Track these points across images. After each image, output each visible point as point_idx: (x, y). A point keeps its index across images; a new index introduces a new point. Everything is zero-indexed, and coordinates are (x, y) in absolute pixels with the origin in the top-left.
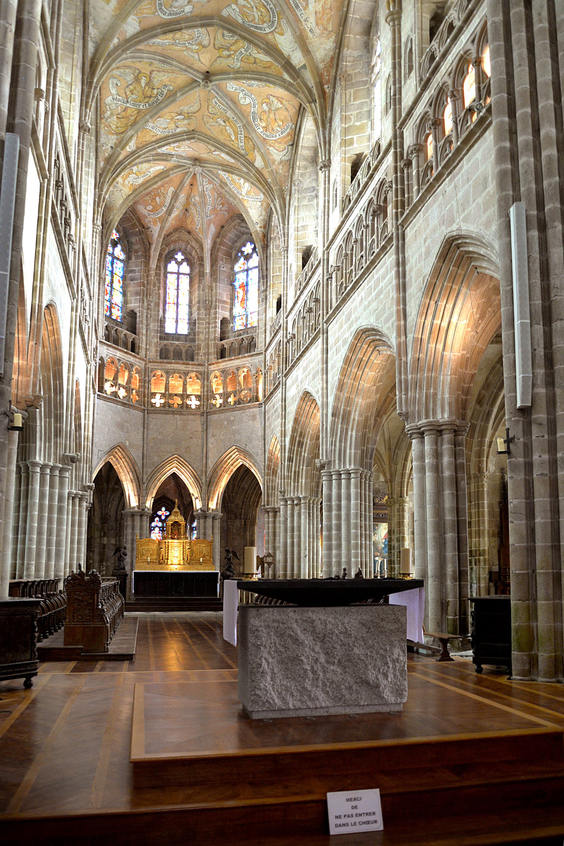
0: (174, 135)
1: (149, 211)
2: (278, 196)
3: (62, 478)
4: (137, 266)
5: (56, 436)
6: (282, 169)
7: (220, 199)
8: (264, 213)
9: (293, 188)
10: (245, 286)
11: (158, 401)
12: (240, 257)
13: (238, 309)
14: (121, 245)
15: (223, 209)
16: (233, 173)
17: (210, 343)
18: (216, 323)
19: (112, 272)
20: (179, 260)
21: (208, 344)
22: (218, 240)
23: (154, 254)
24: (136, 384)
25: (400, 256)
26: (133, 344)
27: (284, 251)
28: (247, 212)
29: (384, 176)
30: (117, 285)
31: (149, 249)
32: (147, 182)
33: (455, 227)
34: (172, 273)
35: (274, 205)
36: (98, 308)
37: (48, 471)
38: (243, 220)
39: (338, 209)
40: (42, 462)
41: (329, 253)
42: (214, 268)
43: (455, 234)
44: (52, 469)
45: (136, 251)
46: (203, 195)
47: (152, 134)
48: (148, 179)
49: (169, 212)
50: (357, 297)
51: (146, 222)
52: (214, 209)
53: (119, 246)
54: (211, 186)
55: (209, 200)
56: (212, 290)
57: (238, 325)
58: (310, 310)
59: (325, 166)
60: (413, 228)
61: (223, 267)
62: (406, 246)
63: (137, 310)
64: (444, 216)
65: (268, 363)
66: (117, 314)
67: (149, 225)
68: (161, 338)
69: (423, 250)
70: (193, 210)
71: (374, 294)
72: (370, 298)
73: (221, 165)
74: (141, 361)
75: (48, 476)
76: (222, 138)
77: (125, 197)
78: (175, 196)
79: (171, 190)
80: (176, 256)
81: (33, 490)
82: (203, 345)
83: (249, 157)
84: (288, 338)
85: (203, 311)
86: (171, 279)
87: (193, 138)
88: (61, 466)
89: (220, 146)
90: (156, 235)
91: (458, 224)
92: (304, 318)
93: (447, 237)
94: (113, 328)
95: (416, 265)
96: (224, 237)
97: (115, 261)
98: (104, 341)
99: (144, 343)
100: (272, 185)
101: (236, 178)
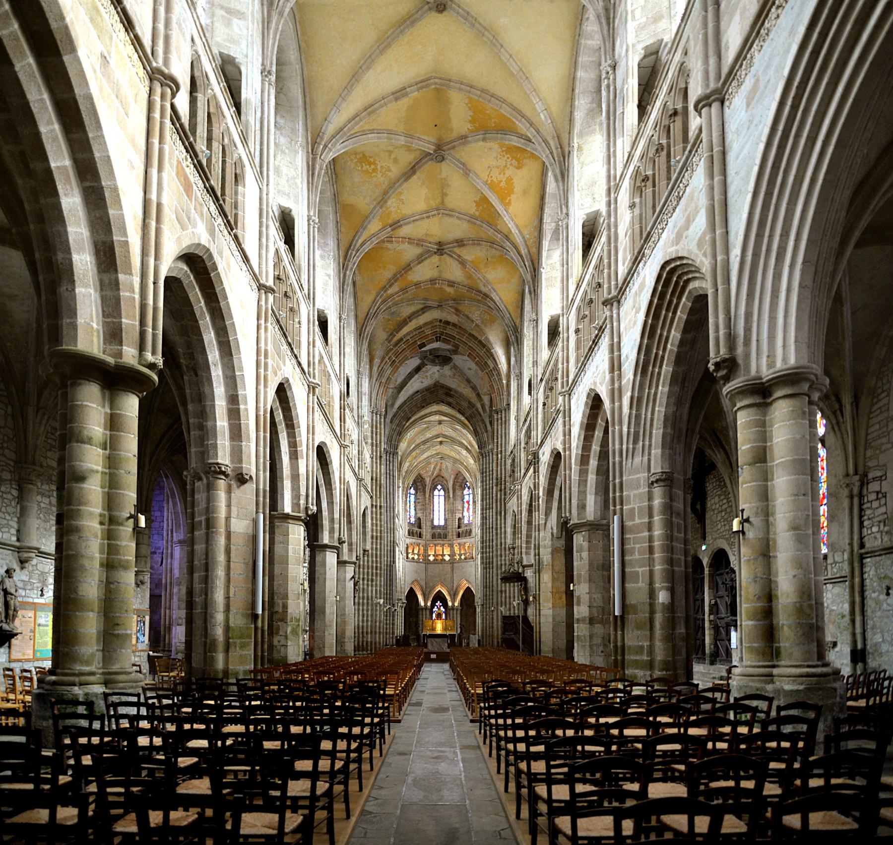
11: (431, 558)
13: (466, 514)
24: (422, 551)
57: (466, 521)
86: (436, 498)
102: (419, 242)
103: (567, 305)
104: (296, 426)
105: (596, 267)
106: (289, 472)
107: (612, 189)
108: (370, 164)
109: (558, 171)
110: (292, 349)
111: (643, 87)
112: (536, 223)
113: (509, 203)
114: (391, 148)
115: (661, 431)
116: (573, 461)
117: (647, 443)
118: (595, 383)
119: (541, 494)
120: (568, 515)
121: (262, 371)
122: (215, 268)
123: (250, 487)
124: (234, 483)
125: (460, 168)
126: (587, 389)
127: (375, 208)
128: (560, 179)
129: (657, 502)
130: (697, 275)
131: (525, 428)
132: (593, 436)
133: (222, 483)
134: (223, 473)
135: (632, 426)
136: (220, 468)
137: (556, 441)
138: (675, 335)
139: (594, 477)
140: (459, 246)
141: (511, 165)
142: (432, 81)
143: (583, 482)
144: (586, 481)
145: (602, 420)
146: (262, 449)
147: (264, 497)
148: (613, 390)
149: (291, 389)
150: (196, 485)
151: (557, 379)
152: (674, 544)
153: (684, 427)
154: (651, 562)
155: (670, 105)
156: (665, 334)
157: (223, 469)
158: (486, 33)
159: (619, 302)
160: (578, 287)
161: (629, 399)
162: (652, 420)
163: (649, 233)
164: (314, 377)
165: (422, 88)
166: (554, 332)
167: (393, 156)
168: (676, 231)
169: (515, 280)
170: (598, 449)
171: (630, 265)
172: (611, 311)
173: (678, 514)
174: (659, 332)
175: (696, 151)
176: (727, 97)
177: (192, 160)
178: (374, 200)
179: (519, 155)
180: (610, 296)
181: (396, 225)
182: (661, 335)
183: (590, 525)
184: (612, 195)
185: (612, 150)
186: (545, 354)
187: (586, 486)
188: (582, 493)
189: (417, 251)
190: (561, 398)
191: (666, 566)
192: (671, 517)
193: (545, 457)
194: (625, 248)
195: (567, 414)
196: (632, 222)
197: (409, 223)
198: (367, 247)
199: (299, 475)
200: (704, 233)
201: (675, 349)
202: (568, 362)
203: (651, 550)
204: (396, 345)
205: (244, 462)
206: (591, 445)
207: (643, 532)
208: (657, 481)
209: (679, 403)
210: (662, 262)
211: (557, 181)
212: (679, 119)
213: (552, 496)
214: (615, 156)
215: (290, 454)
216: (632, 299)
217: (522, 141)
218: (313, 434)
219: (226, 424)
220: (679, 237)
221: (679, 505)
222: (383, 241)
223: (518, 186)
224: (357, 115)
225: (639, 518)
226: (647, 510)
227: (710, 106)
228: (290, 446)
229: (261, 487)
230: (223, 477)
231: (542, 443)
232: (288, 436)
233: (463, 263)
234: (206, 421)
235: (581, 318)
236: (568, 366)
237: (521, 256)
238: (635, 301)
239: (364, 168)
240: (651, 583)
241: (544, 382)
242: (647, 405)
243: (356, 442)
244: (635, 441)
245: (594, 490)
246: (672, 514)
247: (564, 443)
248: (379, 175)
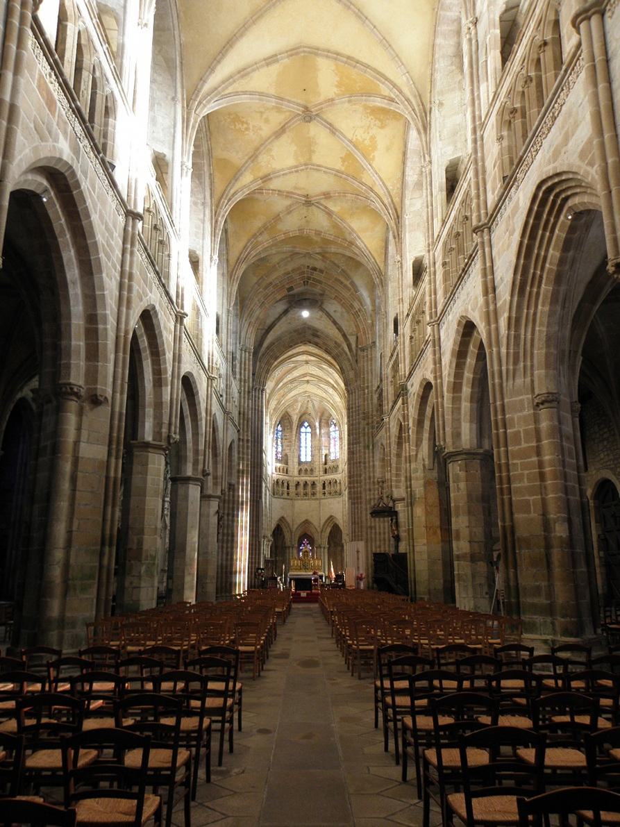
51: (290, 414)
66: (279, 456)
86: (303, 436)
102: (289, 195)
103: (433, 242)
104: (161, 353)
105: (463, 202)
106: (152, 400)
107: (478, 127)
108: (243, 123)
109: (420, 125)
110: (160, 278)
111: (504, 39)
112: (400, 175)
113: (373, 159)
114: (263, 110)
115: (544, 351)
116: (445, 389)
117: (529, 363)
118: (466, 310)
119: (411, 425)
120: (442, 443)
121: (125, 293)
122: (78, 185)
123: (105, 410)
124: (87, 406)
125: (327, 127)
126: (458, 316)
127: (246, 162)
128: (422, 131)
129: (544, 425)
130: (578, 190)
131: (392, 362)
132: (464, 363)
133: (73, 405)
134: (77, 395)
135: (512, 347)
136: (71, 389)
137: (425, 371)
138: (554, 253)
139: (468, 404)
140: (325, 198)
141: (375, 125)
142: (301, 50)
143: (456, 410)
144: (459, 409)
145: (474, 347)
146: (120, 370)
147: (120, 421)
148: (488, 313)
149: (157, 316)
150: (45, 407)
151: (423, 312)
152: (567, 470)
153: (567, 347)
154: (542, 490)
155: (539, 38)
156: (543, 253)
157: (75, 390)
158: (352, 6)
159: (490, 228)
160: (444, 223)
161: (506, 320)
162: (532, 340)
163: (522, 157)
164: (182, 308)
165: (291, 55)
166: (418, 270)
167: (264, 116)
168: (552, 149)
169: (379, 230)
170: (471, 376)
171: (502, 190)
172: (482, 237)
173: (568, 438)
174: (536, 251)
175: (573, 69)
176: (608, 8)
177: (57, 78)
178: (247, 155)
179: (383, 115)
180: (480, 224)
181: (266, 178)
182: (538, 255)
183: (465, 454)
184: (478, 133)
185: (476, 94)
186: (409, 292)
187: (460, 414)
188: (457, 421)
189: (287, 202)
190: (429, 329)
191: (560, 494)
192: (561, 440)
193: (414, 387)
194: (495, 178)
195: (437, 343)
196: (501, 154)
197: (279, 176)
198: (239, 197)
199: (162, 402)
200: (590, 142)
201: (555, 268)
202: (435, 294)
203: (542, 476)
204: (266, 288)
205: (99, 383)
206: (463, 373)
207: (531, 457)
208: (542, 403)
209: (561, 324)
210: (538, 182)
211: (419, 133)
212: (549, 49)
213: (423, 427)
214: (479, 99)
215: (154, 381)
216: (504, 223)
217: (386, 101)
218: (179, 362)
219: (82, 344)
220: (556, 154)
221: (568, 429)
222: (254, 192)
223: (381, 143)
224: (231, 77)
225: (525, 442)
226: (534, 433)
227: (589, 18)
228: (154, 374)
229: (117, 409)
230: (76, 399)
231: (410, 374)
232: (153, 364)
233: (329, 214)
234: (60, 340)
235: (447, 251)
236: (436, 298)
237: (385, 205)
238: (508, 225)
239: (237, 128)
240: (544, 514)
241: (410, 317)
242: (526, 325)
243: (224, 376)
244: (516, 362)
245: (468, 417)
246: (561, 437)
247: (435, 371)
248: (251, 134)
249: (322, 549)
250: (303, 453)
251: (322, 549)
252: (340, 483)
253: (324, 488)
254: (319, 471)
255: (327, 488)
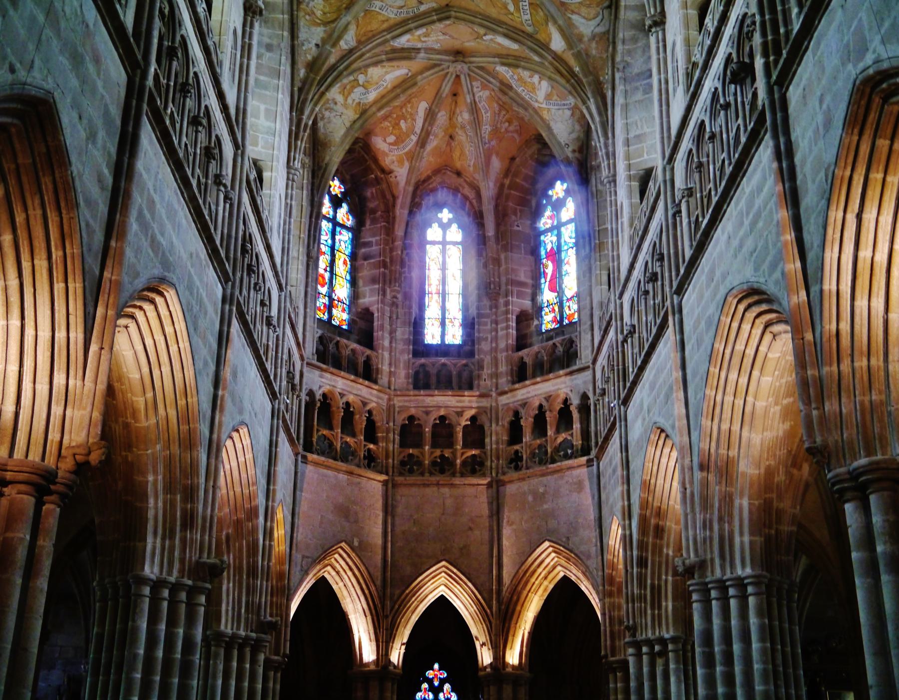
0: (416, 17)
1: (390, 144)
2: (593, 92)
3: (191, 607)
4: (373, 238)
5: (184, 527)
6: (597, 48)
7: (503, 112)
8: (577, 127)
9: (618, 75)
10: (555, 255)
12: (546, 206)
13: (547, 296)
14: (348, 205)
15: (512, 128)
16: (517, 66)
17: (499, 356)
18: (507, 320)
19: (333, 248)
20: (445, 221)
21: (496, 358)
22: (507, 182)
23: (401, 212)
25: (782, 140)
26: (368, 363)
27: (610, 182)
28: (549, 129)
29: (744, 10)
30: (342, 269)
31: (394, 206)
32: (383, 97)
33: (869, 59)
34: (433, 243)
35: (588, 108)
36: (305, 308)
37: (166, 593)
38: (545, 145)
39: (681, 89)
40: (153, 577)
41: (672, 169)
42: (502, 228)
43: (871, 71)
44: (175, 588)
45: (373, 211)
46: (474, 109)
47: (381, 18)
48: (383, 93)
49: (422, 143)
50: (720, 234)
52: (495, 131)
53: (345, 205)
54: (487, 93)
55: (486, 116)
56: (499, 267)
57: (548, 321)
58: (653, 278)
59: (656, 24)
60: (798, 85)
61: (520, 226)
62: (791, 121)
63: (374, 309)
64: (848, 45)
65: (599, 384)
66: (341, 316)
67: (392, 167)
68: (416, 354)
69: (820, 118)
70: (461, 136)
71: (747, 222)
72: (741, 233)
73: (499, 56)
74: (382, 395)
75: (165, 604)
76: (493, 12)
77: (348, 124)
78: (431, 116)
79: (423, 106)
80: (440, 215)
81: (135, 630)
82: (487, 360)
83: (541, 37)
84: (625, 332)
85: (486, 302)
86: (433, 253)
87: (448, 18)
88: (190, 582)
89: (492, 24)
90: (402, 184)
91: (874, 52)
92: (646, 293)
93: (858, 82)
94: (331, 340)
95: (811, 150)
96: (516, 175)
97: (338, 229)
98: (315, 362)
99: (387, 362)
100: (581, 76)
101: (525, 74)
249: (508, 690)
250: (432, 312)
251: (508, 690)
252: (584, 408)
253: (515, 432)
254: (496, 375)
255: (527, 438)
